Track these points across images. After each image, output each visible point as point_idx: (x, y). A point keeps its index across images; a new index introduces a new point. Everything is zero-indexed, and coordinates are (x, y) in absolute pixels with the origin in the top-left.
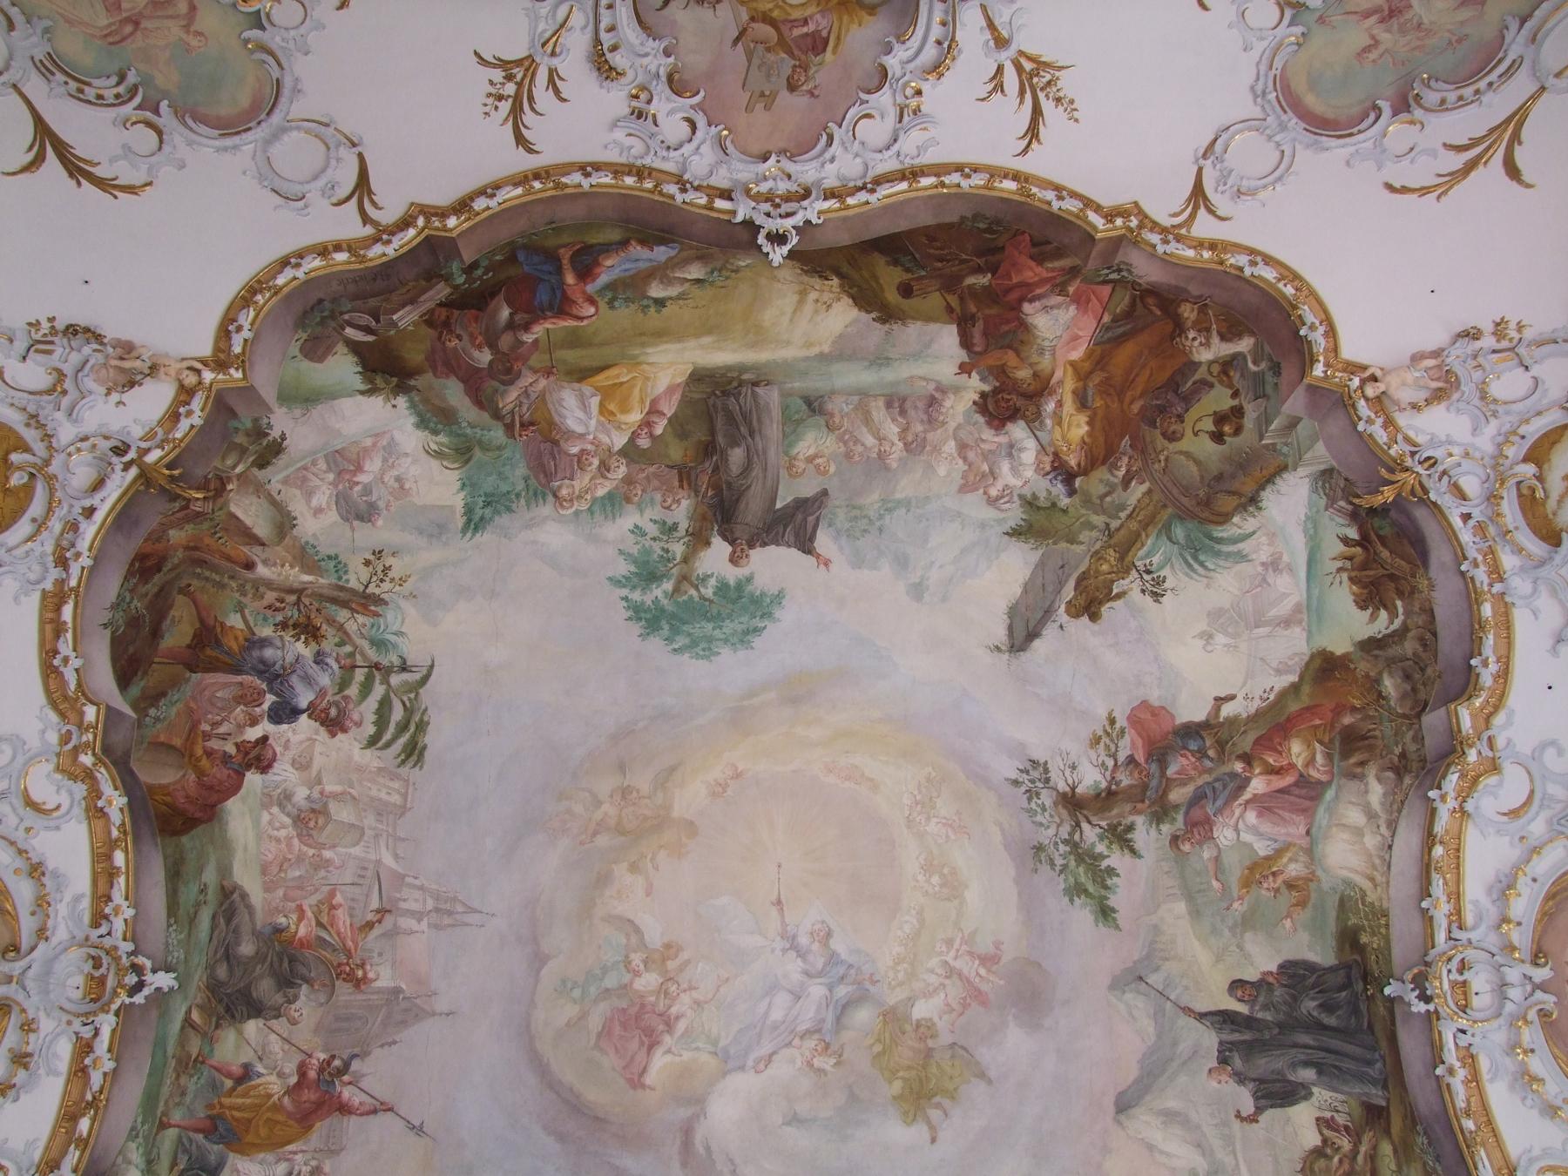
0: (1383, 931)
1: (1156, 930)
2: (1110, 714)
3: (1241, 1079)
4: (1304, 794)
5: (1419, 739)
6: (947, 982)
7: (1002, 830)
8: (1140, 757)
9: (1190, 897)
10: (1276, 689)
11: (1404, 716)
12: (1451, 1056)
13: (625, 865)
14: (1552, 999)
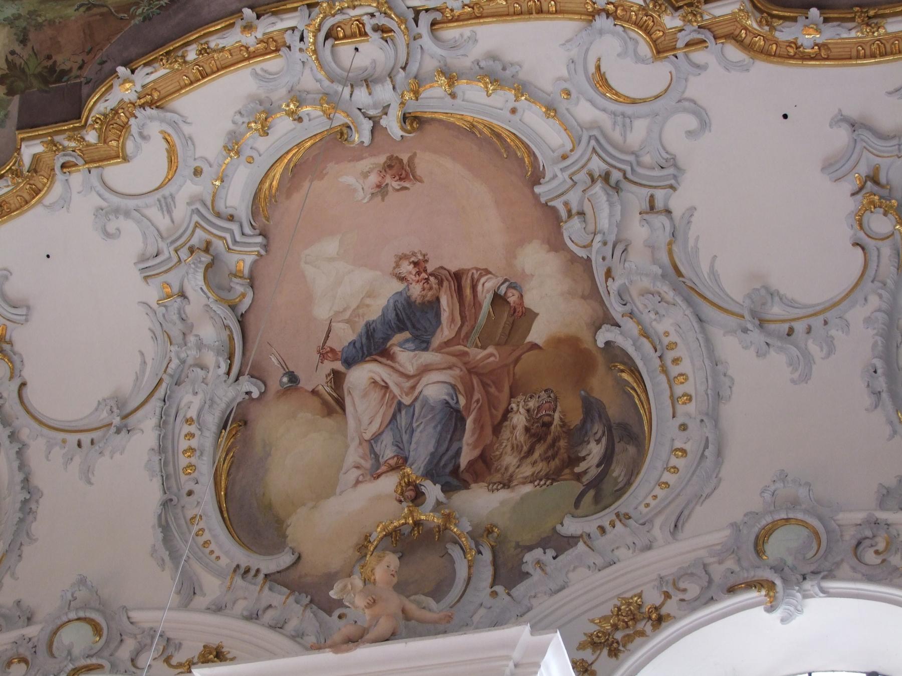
12: (268, 26)
14: (367, 140)
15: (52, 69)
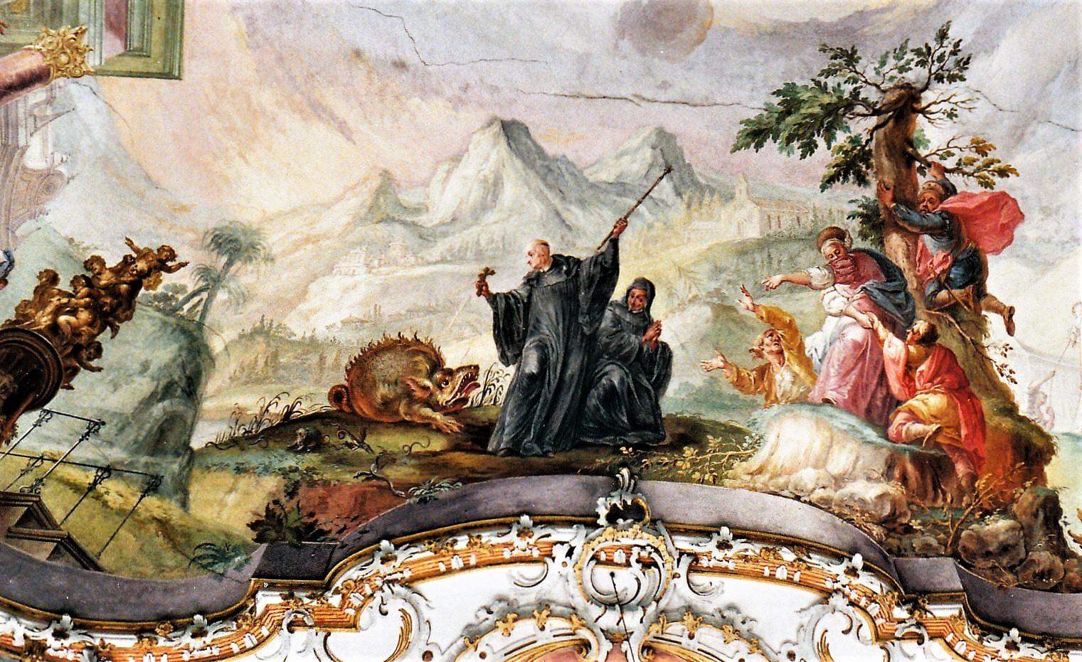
0: (697, 475)
1: (729, 197)
2: (1014, 171)
3: (533, 280)
4: (874, 402)
5: (927, 551)
8: (951, 203)
9: (764, 244)
10: (1011, 386)
11: (957, 537)
15: (310, 527)
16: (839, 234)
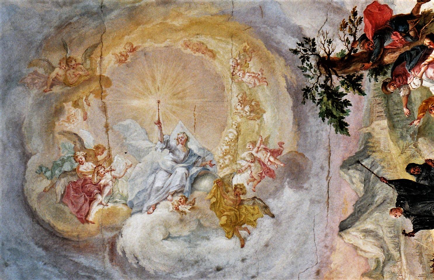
1: (369, 134)
2: (354, 9)
3: (407, 214)
6: (252, 165)
7: (287, 80)
8: (370, 36)
9: (390, 118)
13: (71, 103)
16: (385, 85)
